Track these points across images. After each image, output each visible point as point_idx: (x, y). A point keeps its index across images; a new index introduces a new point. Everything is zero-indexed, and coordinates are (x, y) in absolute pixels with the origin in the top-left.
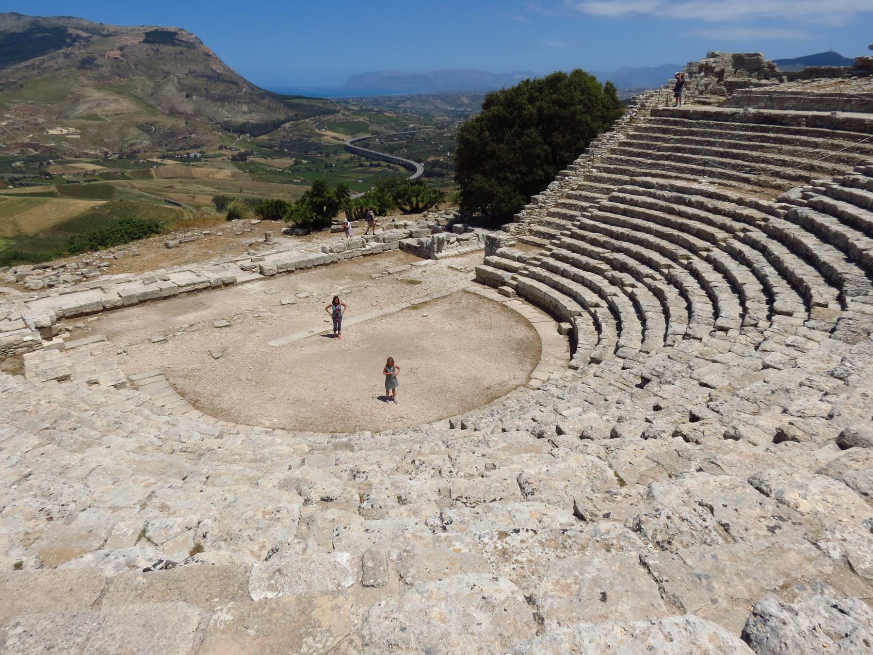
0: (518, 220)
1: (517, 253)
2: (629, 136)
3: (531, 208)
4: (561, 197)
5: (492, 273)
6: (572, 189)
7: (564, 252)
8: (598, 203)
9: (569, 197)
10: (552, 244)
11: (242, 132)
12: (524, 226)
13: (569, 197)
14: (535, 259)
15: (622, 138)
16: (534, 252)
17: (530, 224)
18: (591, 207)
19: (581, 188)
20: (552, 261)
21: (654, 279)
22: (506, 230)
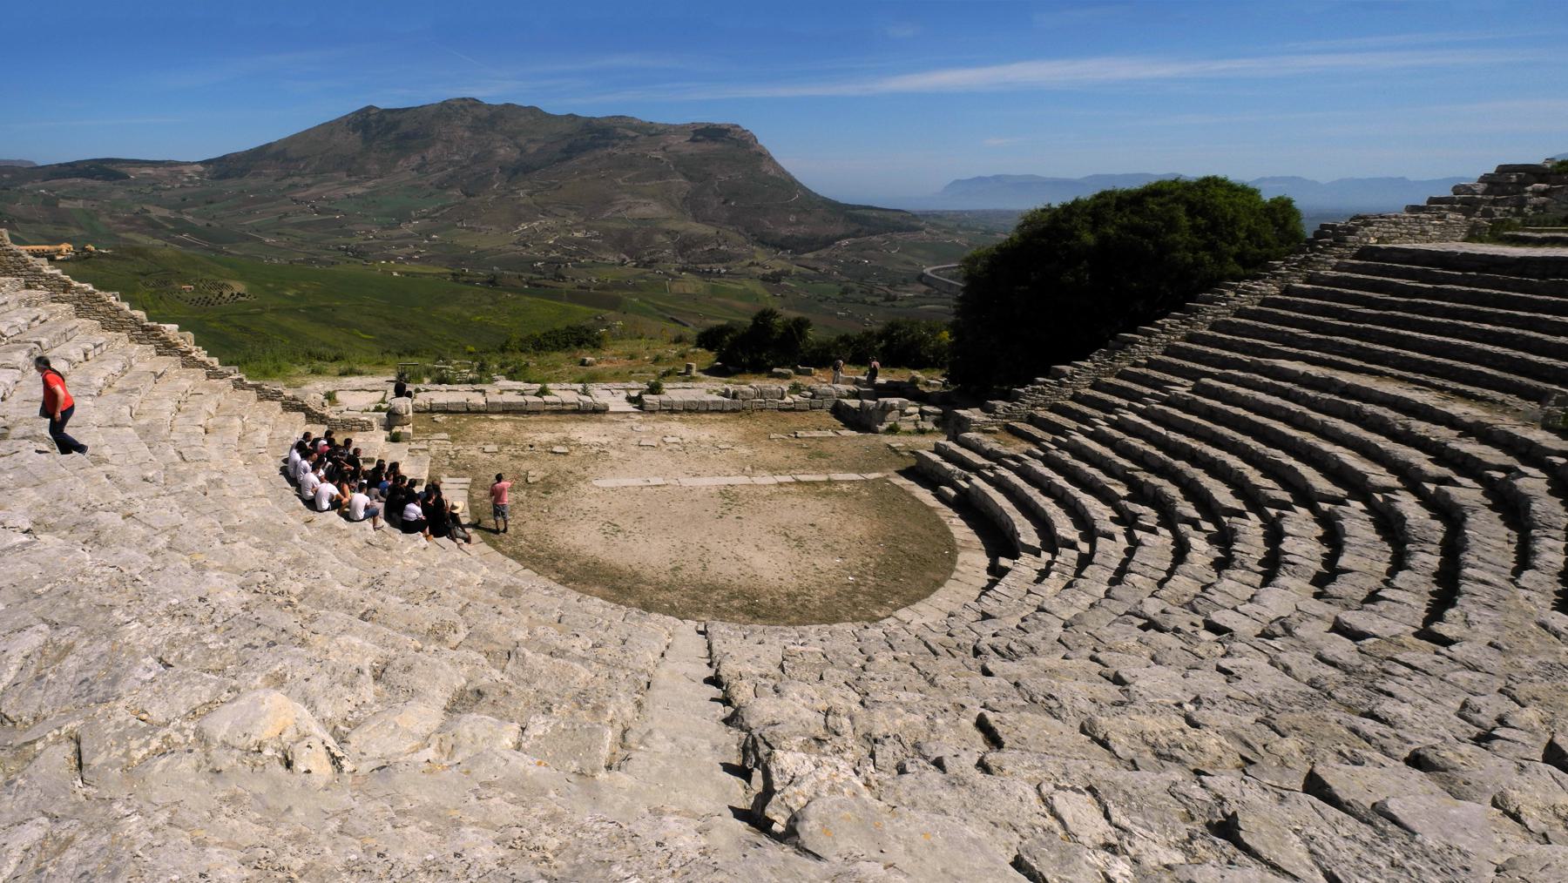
0: (1007, 396)
1: (990, 443)
2: (1287, 291)
3: (1044, 384)
4: (1110, 374)
5: (936, 464)
6: (1136, 365)
7: (1066, 456)
8: (1167, 391)
9: (1123, 375)
10: (1054, 442)
11: (783, 248)
12: (1023, 408)
13: (1123, 375)
14: (1015, 458)
15: (1272, 290)
16: (1017, 448)
17: (1034, 406)
18: (1152, 396)
19: (1152, 364)
20: (1039, 467)
21: (1197, 527)
22: (988, 410)
